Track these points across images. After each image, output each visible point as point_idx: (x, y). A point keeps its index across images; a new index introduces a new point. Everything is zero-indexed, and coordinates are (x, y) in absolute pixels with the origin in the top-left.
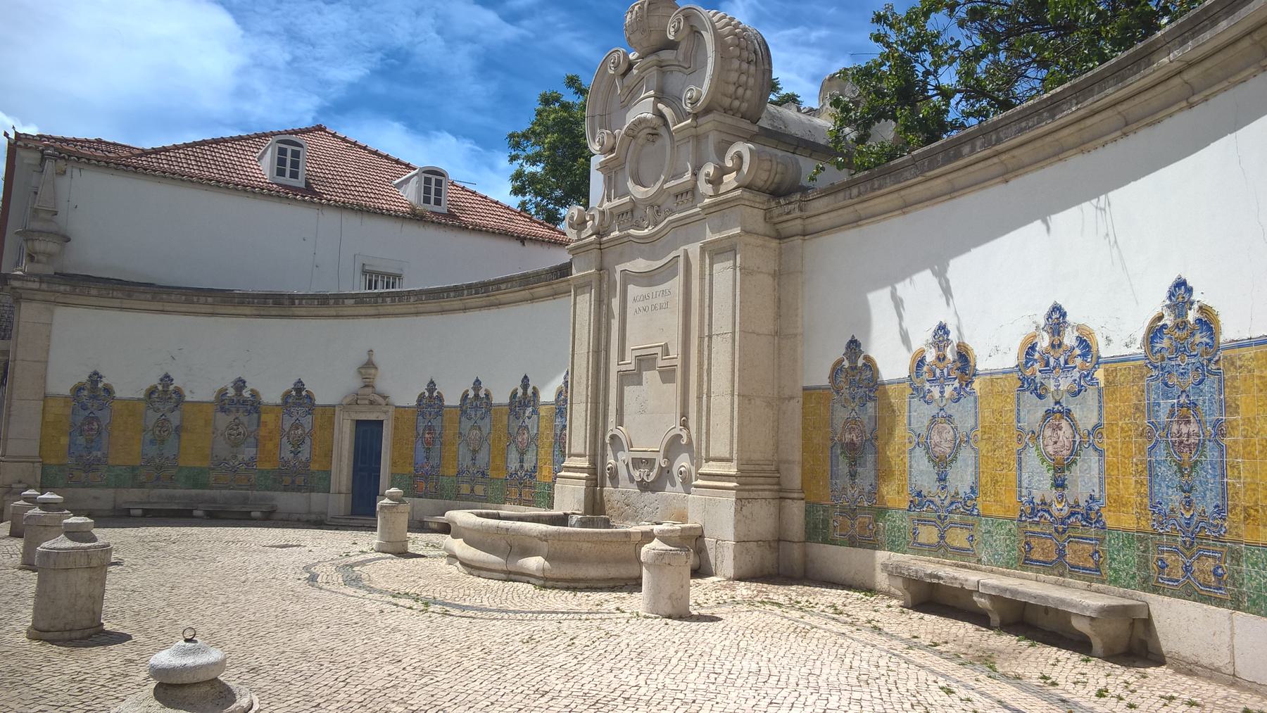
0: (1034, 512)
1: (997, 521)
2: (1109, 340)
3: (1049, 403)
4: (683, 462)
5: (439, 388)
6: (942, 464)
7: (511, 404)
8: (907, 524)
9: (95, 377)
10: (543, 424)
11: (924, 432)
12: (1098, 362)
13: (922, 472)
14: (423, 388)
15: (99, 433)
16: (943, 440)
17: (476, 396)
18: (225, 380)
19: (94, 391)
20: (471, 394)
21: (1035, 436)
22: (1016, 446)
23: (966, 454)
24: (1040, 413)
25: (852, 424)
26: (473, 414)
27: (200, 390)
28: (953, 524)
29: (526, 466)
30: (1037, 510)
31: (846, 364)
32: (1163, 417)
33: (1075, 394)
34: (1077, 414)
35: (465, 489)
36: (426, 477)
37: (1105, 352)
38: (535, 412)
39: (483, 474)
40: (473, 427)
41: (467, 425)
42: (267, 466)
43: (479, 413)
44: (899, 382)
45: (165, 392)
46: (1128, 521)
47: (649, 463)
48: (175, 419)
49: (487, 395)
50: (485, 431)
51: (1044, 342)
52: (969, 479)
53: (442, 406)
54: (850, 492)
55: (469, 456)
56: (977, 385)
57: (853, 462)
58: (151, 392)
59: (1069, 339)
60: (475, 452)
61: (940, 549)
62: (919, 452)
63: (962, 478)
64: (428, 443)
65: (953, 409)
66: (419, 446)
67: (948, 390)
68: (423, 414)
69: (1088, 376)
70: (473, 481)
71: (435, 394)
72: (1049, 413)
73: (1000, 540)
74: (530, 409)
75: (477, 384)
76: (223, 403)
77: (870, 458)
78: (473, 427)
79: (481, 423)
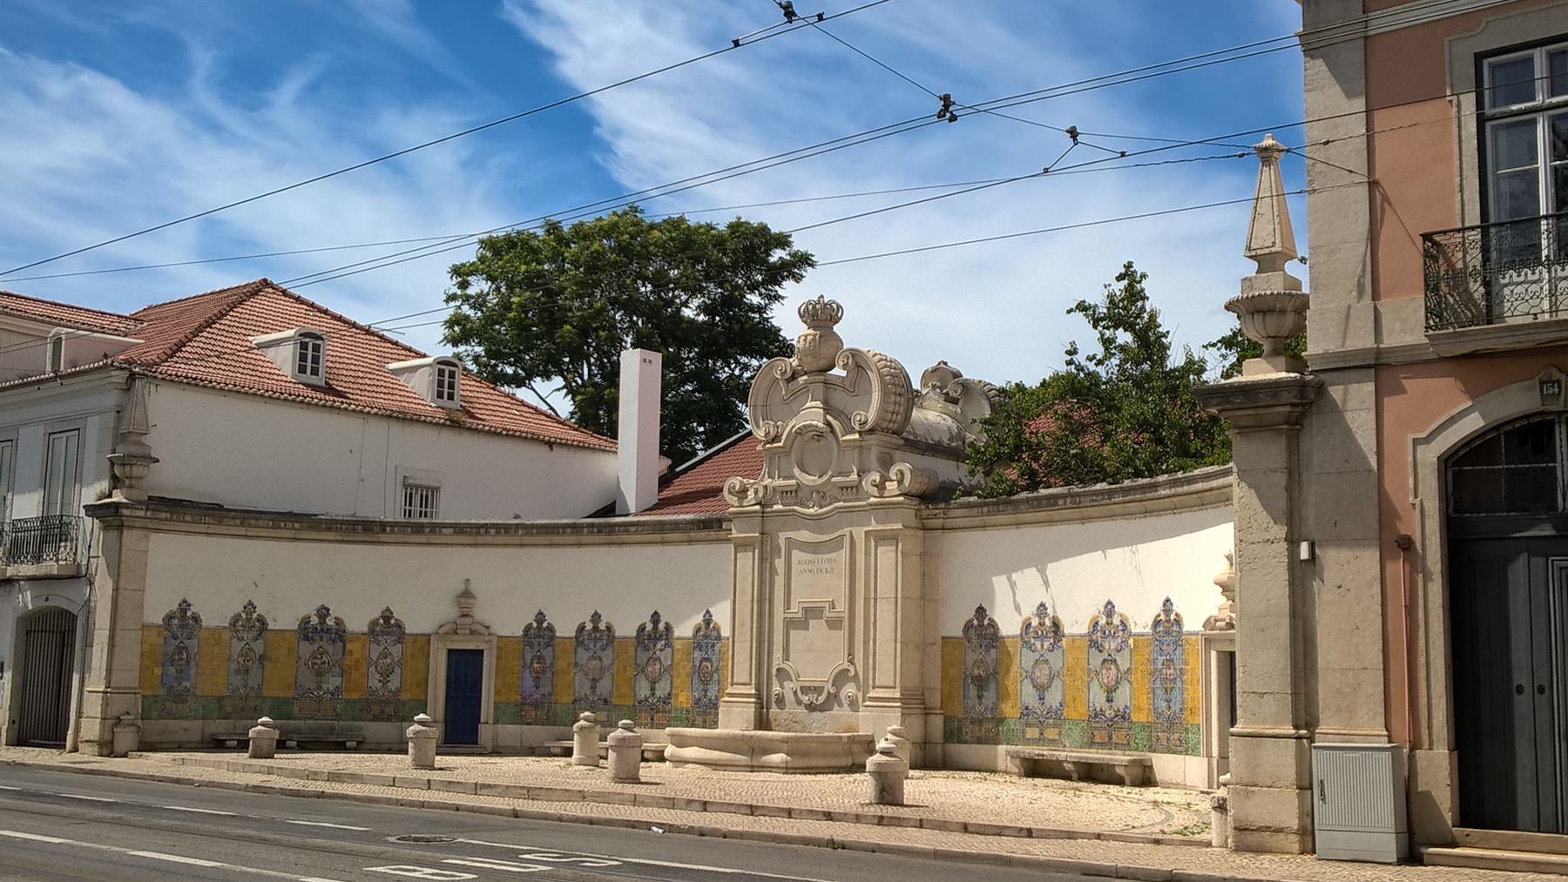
1: (1075, 722)
4: (849, 690)
6: (1042, 689)
9: (185, 605)
13: (1029, 695)
14: (531, 619)
15: (188, 662)
16: (1042, 675)
17: (595, 628)
18: (310, 609)
19: (183, 620)
20: (589, 626)
23: (1057, 683)
27: (284, 619)
36: (535, 705)
40: (592, 658)
42: (354, 696)
45: (249, 620)
47: (818, 690)
48: (258, 647)
49: (609, 628)
50: (607, 662)
52: (1059, 699)
55: (587, 685)
58: (235, 620)
60: (594, 681)
61: (1040, 741)
63: (1054, 698)
65: (1048, 656)
67: (1046, 644)
68: (531, 645)
73: (1076, 733)
75: (596, 617)
76: (307, 631)
78: (592, 658)
79: (599, 653)
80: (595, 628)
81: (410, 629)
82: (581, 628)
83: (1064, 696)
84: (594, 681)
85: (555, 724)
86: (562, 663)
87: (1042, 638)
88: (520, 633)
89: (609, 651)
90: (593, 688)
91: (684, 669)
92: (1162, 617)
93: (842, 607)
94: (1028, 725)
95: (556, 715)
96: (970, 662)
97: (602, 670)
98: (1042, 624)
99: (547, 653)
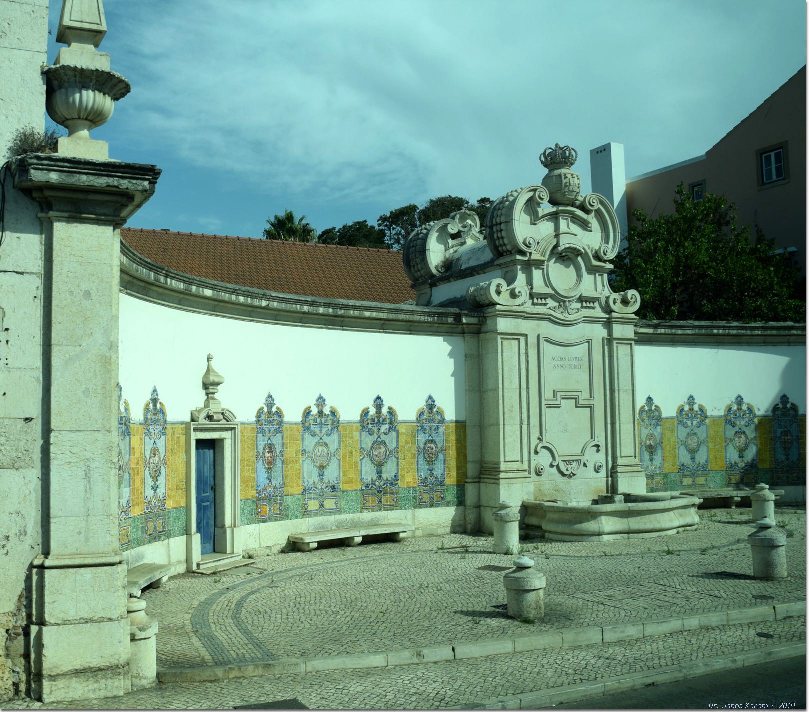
0: (732, 466)
2: (759, 410)
3: (737, 429)
5: (279, 403)
6: (693, 452)
7: (362, 421)
8: (678, 478)
10: (403, 440)
11: (684, 439)
12: (755, 416)
17: (321, 413)
20: (315, 411)
21: (732, 440)
22: (724, 444)
24: (734, 432)
25: (650, 436)
26: (318, 430)
28: (699, 475)
29: (385, 476)
30: (732, 466)
31: (647, 408)
32: (779, 434)
33: (747, 426)
34: (748, 433)
35: (313, 505)
36: (269, 499)
37: (758, 413)
38: (393, 427)
39: (334, 488)
41: (310, 442)
43: (324, 430)
44: (672, 418)
46: (767, 465)
49: (333, 413)
50: (333, 447)
51: (735, 407)
52: (705, 457)
53: (281, 423)
54: (650, 468)
55: (316, 472)
56: (707, 421)
57: (652, 454)
59: (745, 407)
60: (322, 467)
62: (683, 448)
63: (702, 457)
64: (269, 463)
65: (696, 430)
66: (261, 465)
67: (695, 423)
68: (262, 431)
69: (752, 420)
70: (322, 495)
71: (274, 409)
72: (736, 432)
73: (718, 478)
74: (387, 426)
75: (321, 401)
77: (660, 451)
78: (319, 444)
79: (326, 439)
80: (321, 413)
81: (170, 418)
82: (307, 413)
83: (708, 456)
84: (322, 467)
85: (287, 517)
86: (290, 452)
87: (692, 418)
88: (253, 419)
89: (335, 436)
90: (321, 475)
91: (408, 452)
92: (781, 406)
93: (586, 395)
94: (685, 476)
95: (287, 508)
96: (644, 436)
97: (329, 456)
98: (692, 409)
99: (277, 440)
